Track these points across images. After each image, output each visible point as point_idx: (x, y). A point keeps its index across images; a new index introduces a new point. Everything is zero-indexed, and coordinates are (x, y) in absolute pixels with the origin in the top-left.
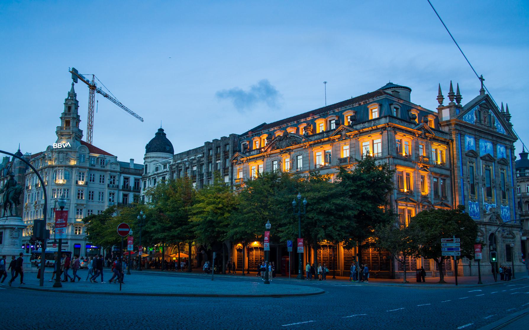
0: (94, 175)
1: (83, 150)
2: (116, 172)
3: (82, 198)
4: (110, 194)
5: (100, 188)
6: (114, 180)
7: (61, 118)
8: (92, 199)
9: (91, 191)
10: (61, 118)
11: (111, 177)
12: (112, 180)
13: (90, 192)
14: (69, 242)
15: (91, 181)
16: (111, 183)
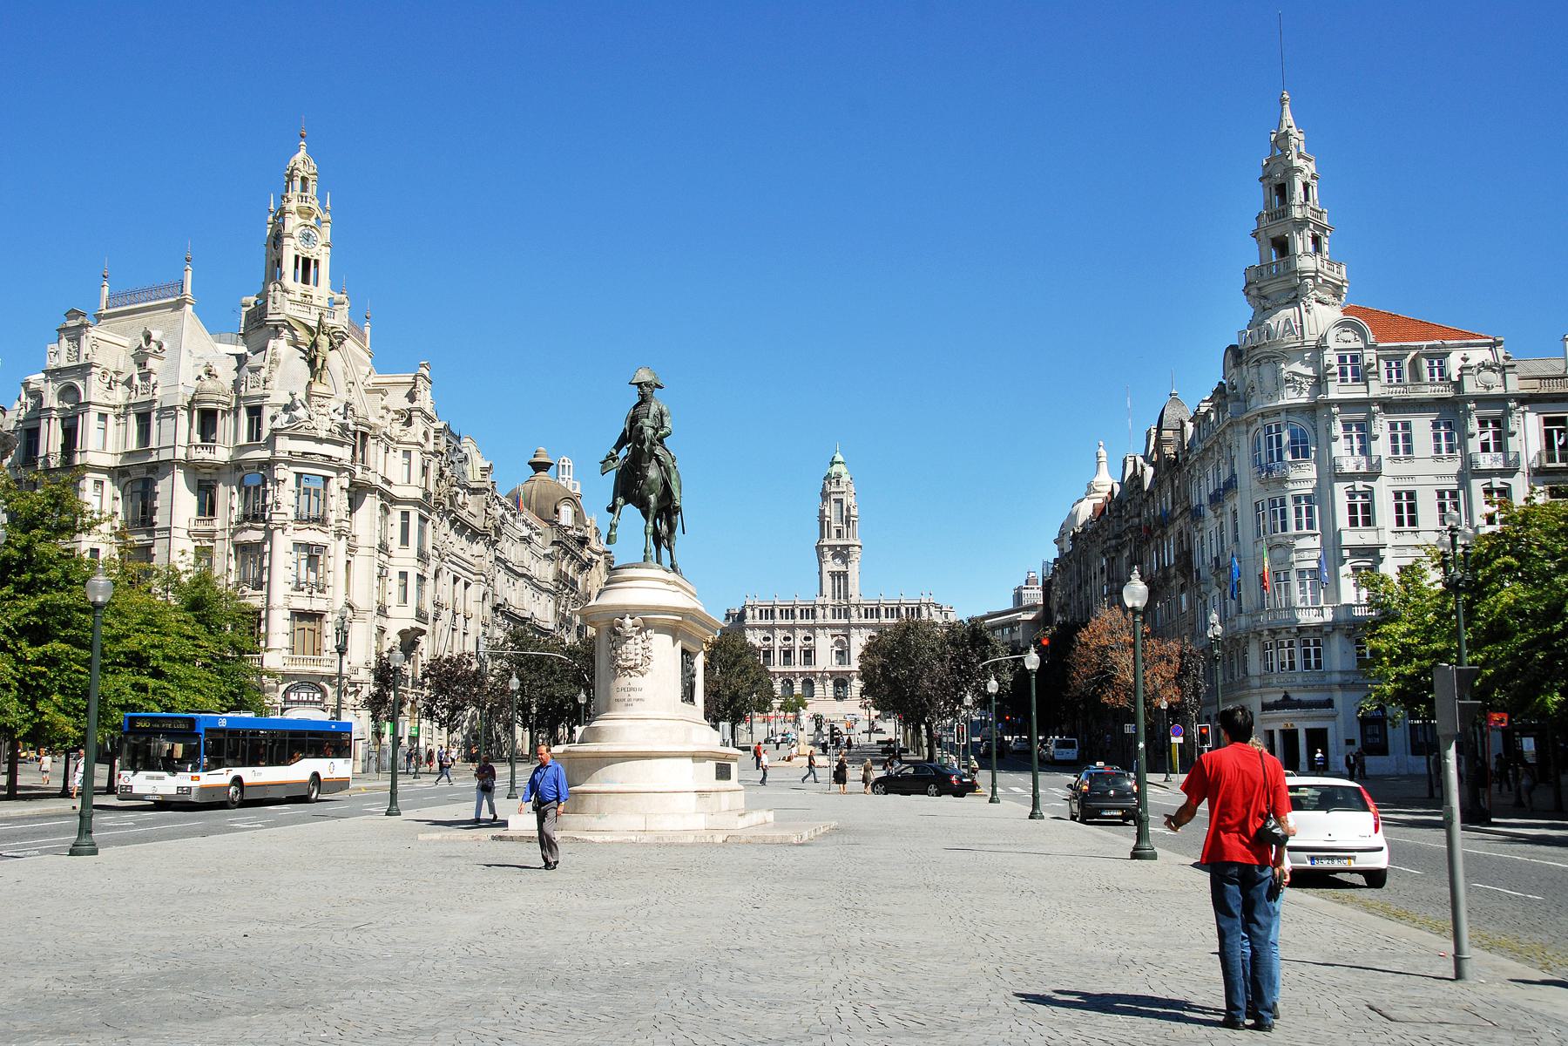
0: (1406, 426)
1: (1349, 336)
2: (1501, 400)
3: (1368, 522)
4: (1488, 492)
5: (1437, 476)
6: (1497, 435)
7: (1255, 235)
8: (1413, 522)
9: (1405, 486)
10: (1255, 235)
11: (1483, 423)
12: (1489, 435)
13: (1398, 495)
14: (1338, 697)
15: (1395, 450)
16: (1485, 447)
